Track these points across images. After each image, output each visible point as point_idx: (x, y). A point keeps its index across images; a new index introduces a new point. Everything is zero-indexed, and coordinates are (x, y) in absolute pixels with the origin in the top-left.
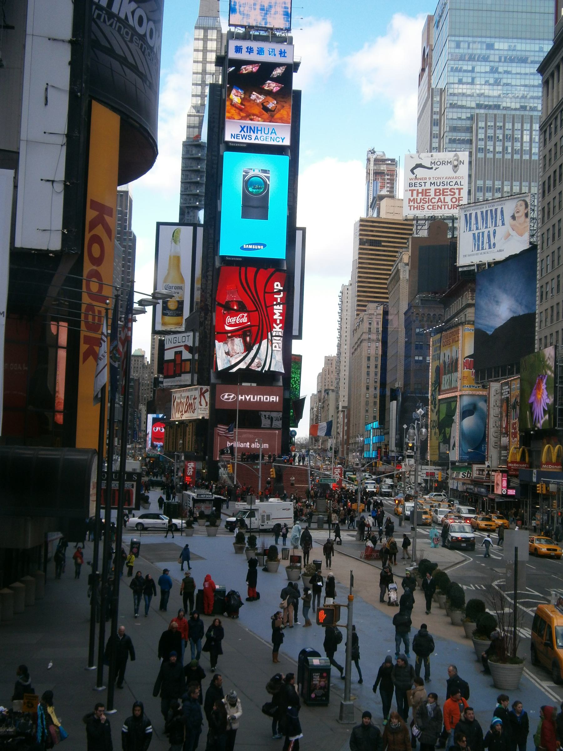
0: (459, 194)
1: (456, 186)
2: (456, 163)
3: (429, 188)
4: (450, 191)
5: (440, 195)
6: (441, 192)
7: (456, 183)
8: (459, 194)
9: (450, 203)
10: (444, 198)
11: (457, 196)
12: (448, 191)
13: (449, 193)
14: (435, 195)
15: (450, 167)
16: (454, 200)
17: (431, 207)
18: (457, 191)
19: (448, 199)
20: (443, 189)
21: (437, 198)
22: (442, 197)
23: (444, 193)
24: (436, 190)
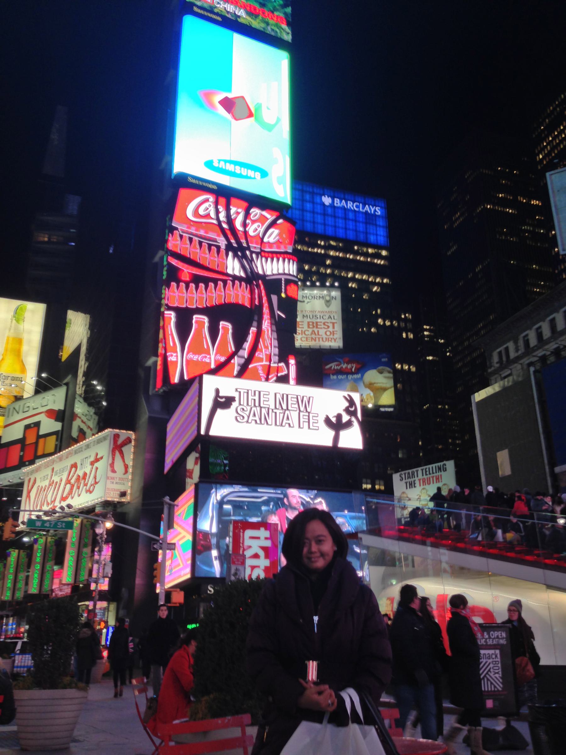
0: (334, 328)
1: (330, 320)
2: (328, 298)
3: (303, 320)
4: (324, 324)
5: (314, 327)
6: (315, 325)
7: (330, 317)
8: (334, 328)
9: (324, 336)
10: (318, 331)
11: (331, 329)
12: (322, 324)
13: (323, 326)
14: (309, 327)
15: (322, 302)
16: (328, 333)
17: (305, 339)
18: (331, 325)
19: (322, 332)
20: (317, 323)
21: (310, 330)
22: (316, 330)
23: (316, 325)
24: (308, 323)
